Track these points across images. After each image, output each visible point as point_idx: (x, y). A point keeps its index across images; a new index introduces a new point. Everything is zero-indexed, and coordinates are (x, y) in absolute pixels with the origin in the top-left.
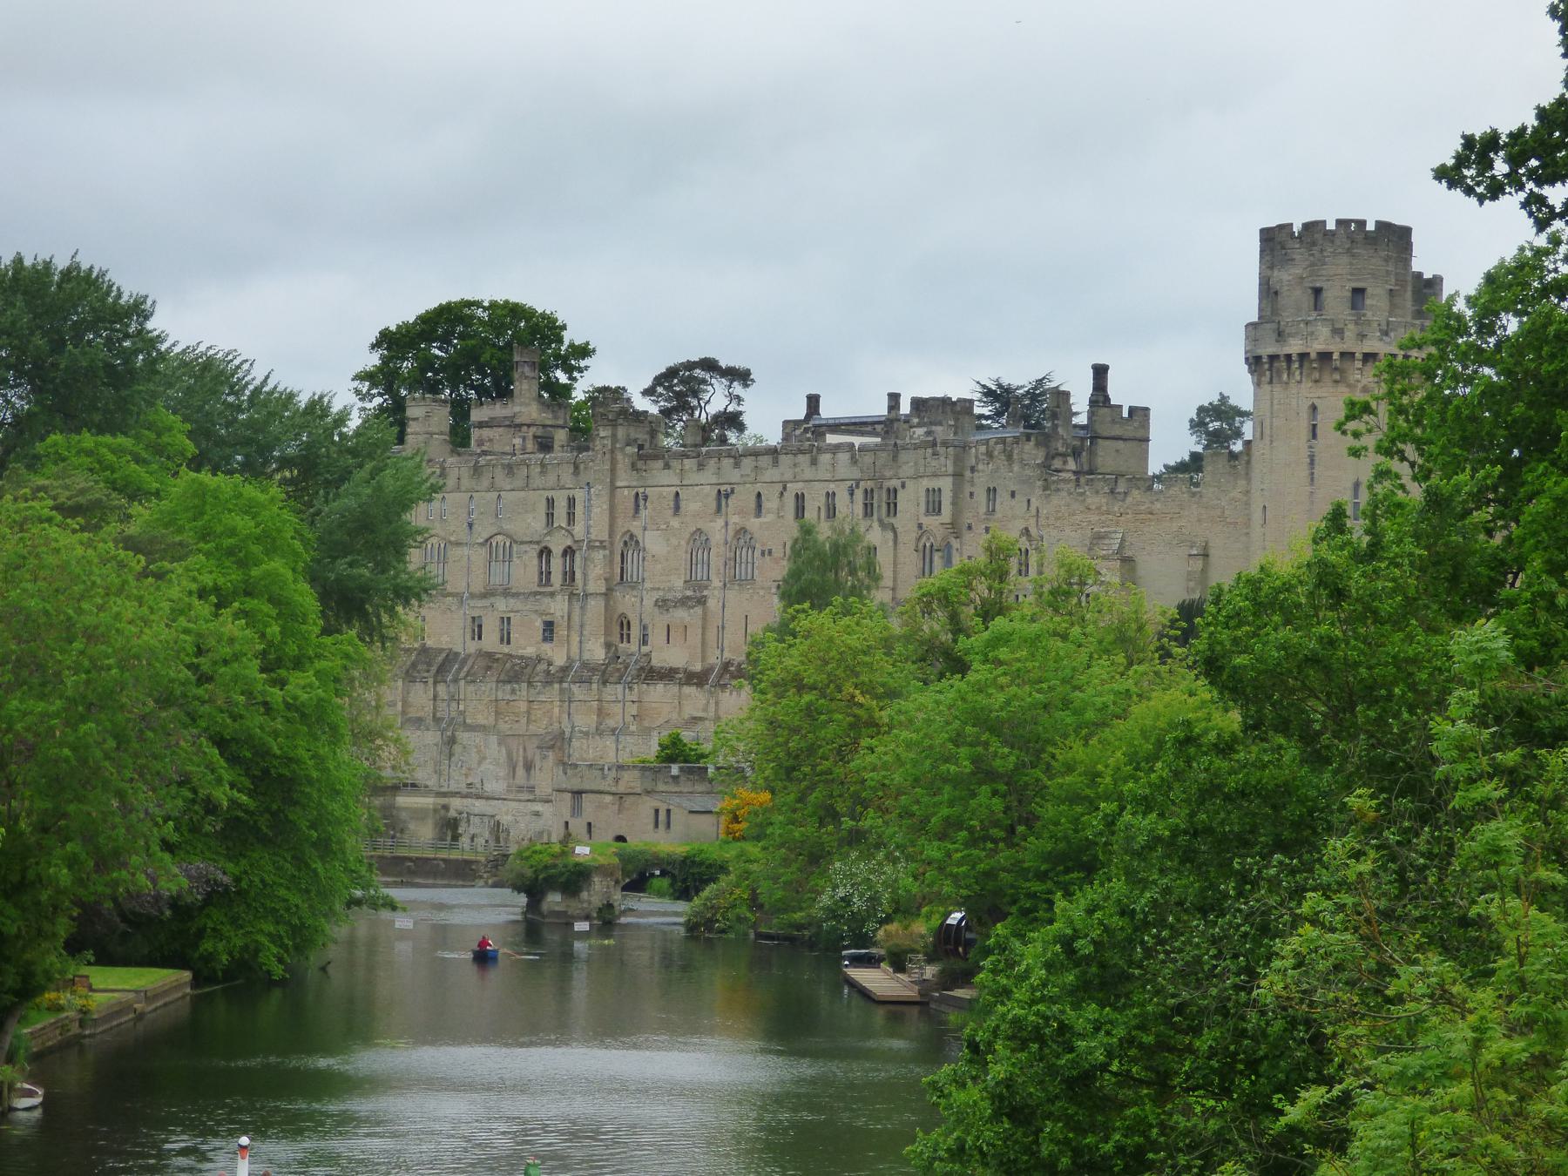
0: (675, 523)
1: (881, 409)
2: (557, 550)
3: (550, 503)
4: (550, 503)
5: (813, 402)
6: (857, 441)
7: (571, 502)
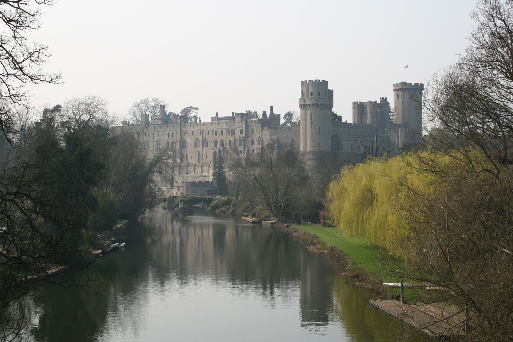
0: (192, 137)
1: (231, 115)
2: (170, 142)
3: (169, 134)
4: (169, 134)
5: (217, 114)
6: (227, 121)
7: (173, 133)
